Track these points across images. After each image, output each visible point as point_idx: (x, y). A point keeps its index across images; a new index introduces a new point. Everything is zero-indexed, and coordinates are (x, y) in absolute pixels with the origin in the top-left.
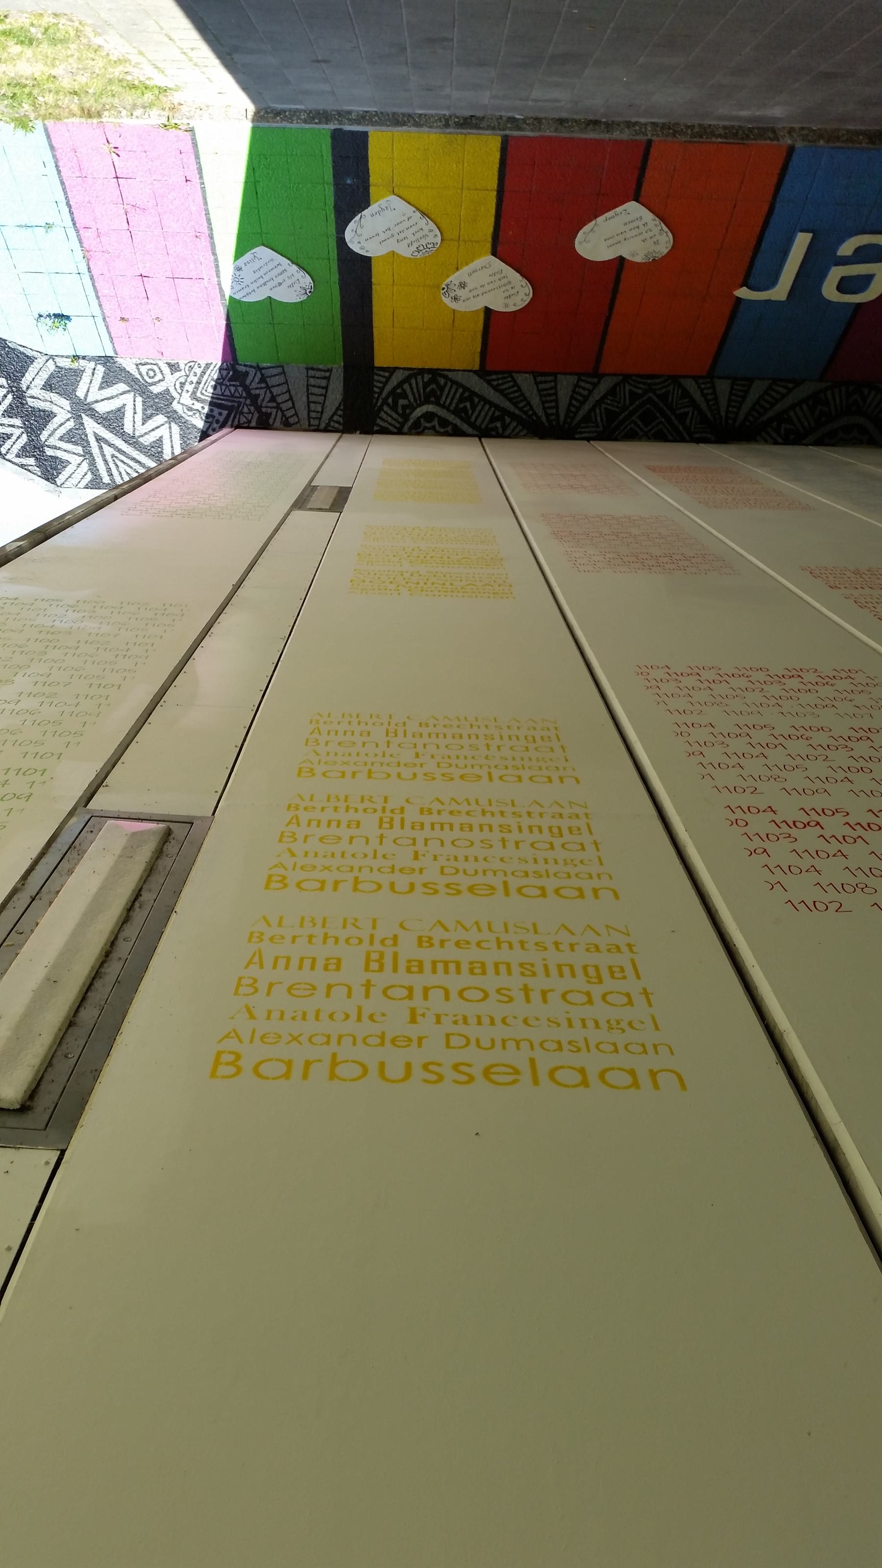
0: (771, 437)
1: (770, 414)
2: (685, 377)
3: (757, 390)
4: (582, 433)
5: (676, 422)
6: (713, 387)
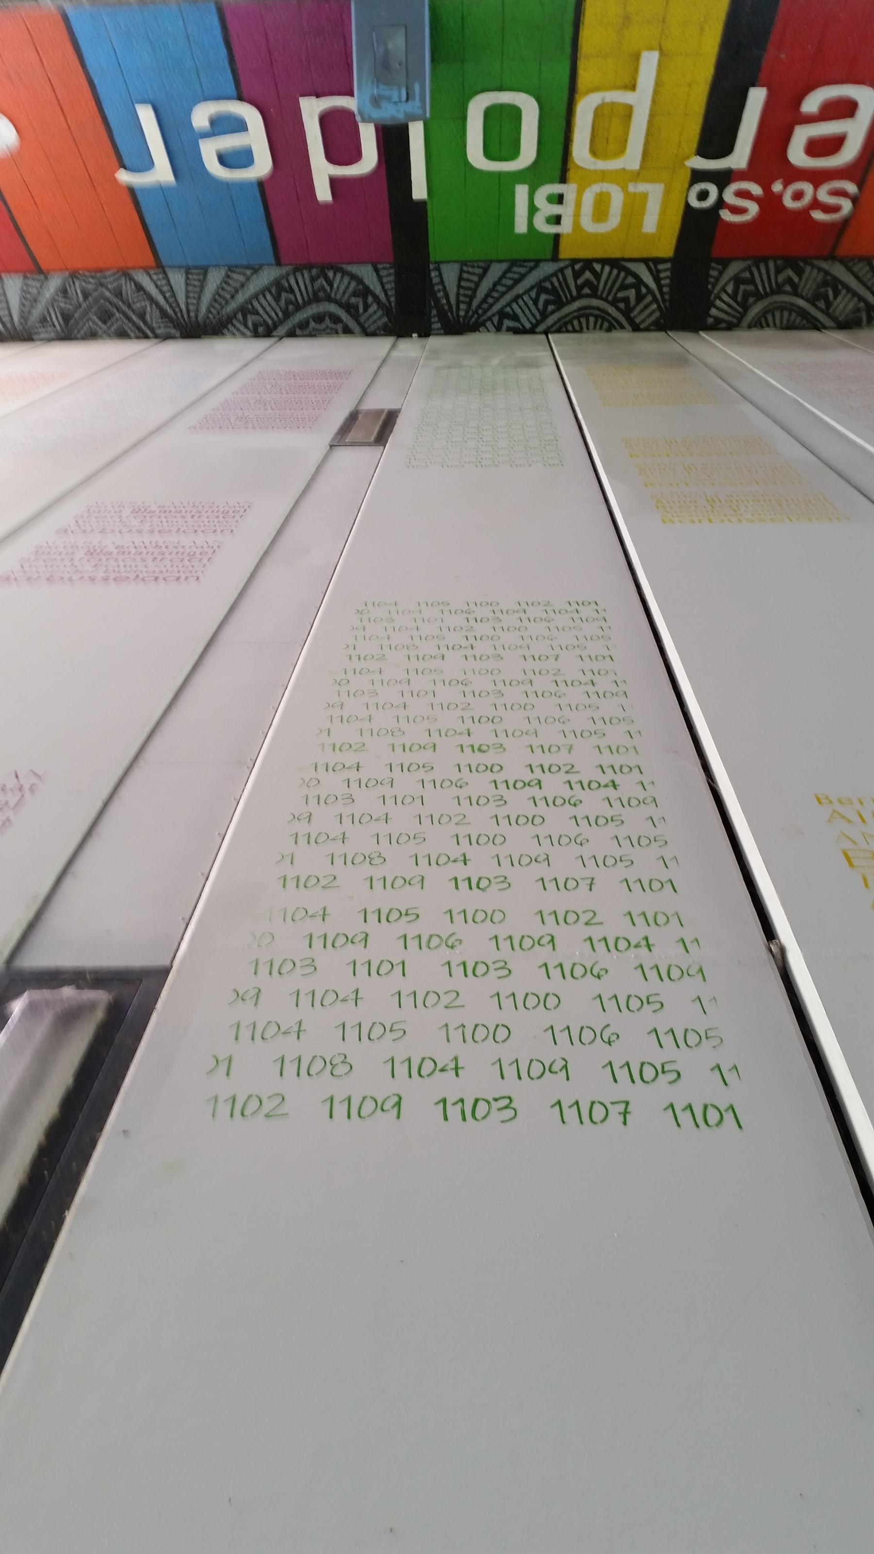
0: (238, 330)
1: (233, 305)
2: (134, 268)
3: (214, 279)
5: (134, 318)
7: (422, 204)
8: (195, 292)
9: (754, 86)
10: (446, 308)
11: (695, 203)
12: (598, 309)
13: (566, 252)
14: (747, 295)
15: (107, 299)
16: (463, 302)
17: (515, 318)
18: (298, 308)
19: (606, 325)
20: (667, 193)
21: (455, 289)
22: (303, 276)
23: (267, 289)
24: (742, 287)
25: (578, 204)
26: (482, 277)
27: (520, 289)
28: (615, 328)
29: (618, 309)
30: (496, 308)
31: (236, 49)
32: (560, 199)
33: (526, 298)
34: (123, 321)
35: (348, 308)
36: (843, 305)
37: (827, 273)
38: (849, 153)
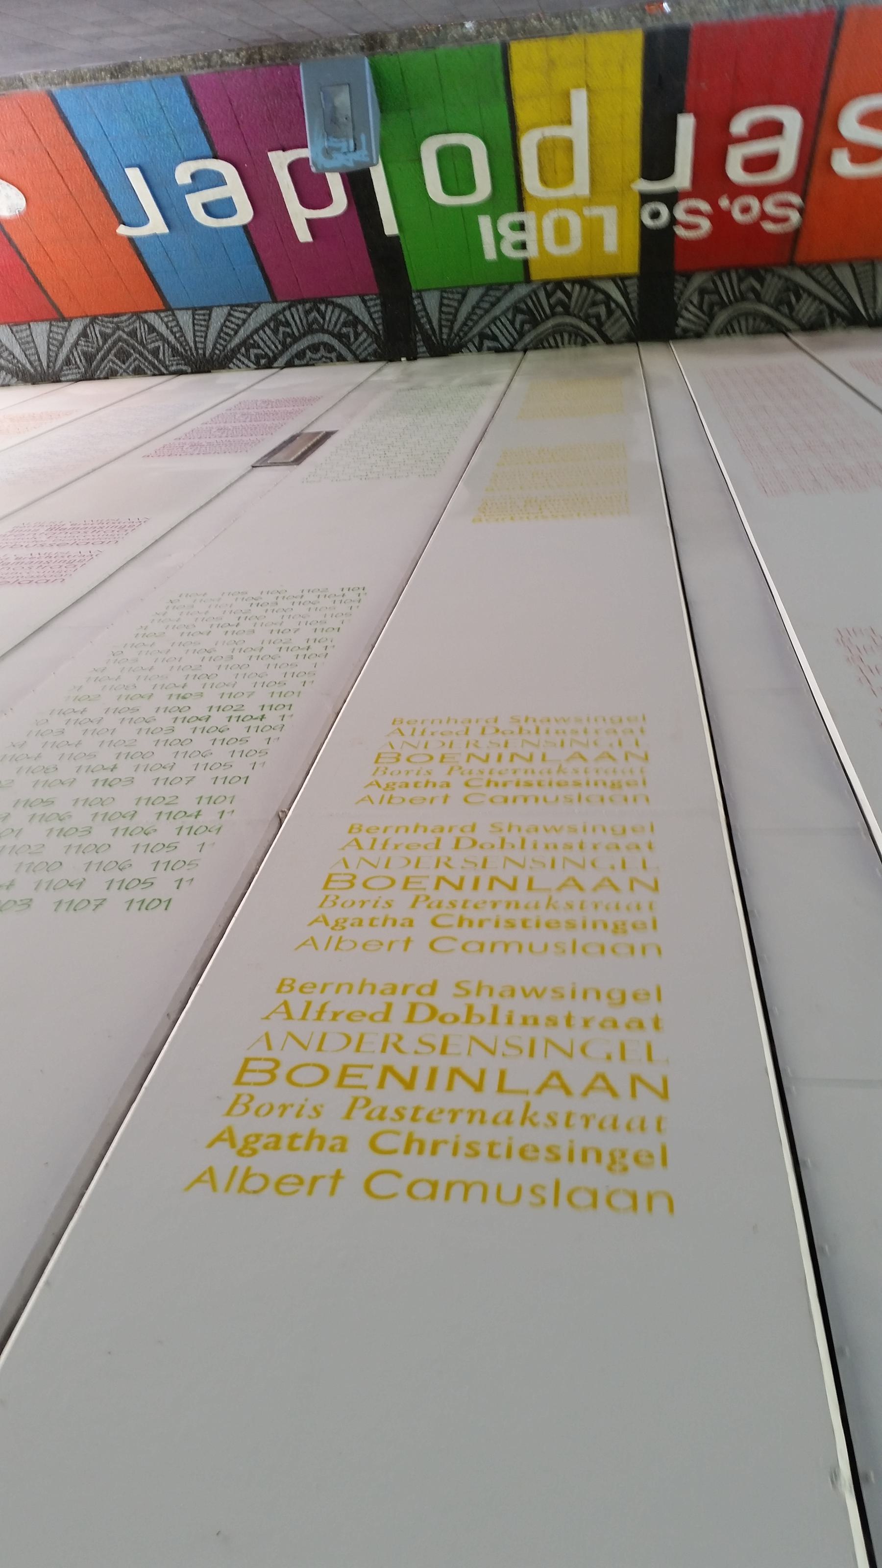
0: (243, 363)
1: (237, 341)
2: (146, 312)
3: (218, 316)
4: (65, 375)
5: (150, 357)
6: (175, 319)
7: (395, 239)
8: (201, 331)
9: (681, 112)
10: (430, 332)
11: (648, 222)
12: (572, 326)
13: (537, 274)
14: (711, 306)
15: (125, 341)
16: (446, 326)
17: (495, 338)
18: (296, 340)
19: (579, 340)
20: (621, 214)
21: (437, 314)
22: (298, 310)
23: (266, 323)
24: (706, 297)
25: (540, 230)
26: (460, 302)
27: (497, 311)
28: (588, 342)
29: (589, 324)
30: (476, 330)
31: (205, 117)
32: (522, 227)
33: (503, 319)
34: (140, 360)
35: (340, 337)
36: (806, 309)
37: (787, 279)
38: (786, 167)
